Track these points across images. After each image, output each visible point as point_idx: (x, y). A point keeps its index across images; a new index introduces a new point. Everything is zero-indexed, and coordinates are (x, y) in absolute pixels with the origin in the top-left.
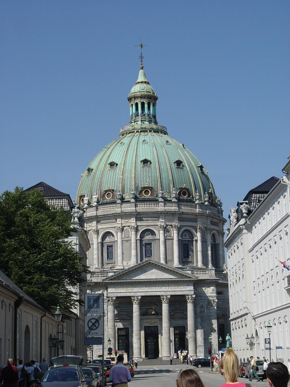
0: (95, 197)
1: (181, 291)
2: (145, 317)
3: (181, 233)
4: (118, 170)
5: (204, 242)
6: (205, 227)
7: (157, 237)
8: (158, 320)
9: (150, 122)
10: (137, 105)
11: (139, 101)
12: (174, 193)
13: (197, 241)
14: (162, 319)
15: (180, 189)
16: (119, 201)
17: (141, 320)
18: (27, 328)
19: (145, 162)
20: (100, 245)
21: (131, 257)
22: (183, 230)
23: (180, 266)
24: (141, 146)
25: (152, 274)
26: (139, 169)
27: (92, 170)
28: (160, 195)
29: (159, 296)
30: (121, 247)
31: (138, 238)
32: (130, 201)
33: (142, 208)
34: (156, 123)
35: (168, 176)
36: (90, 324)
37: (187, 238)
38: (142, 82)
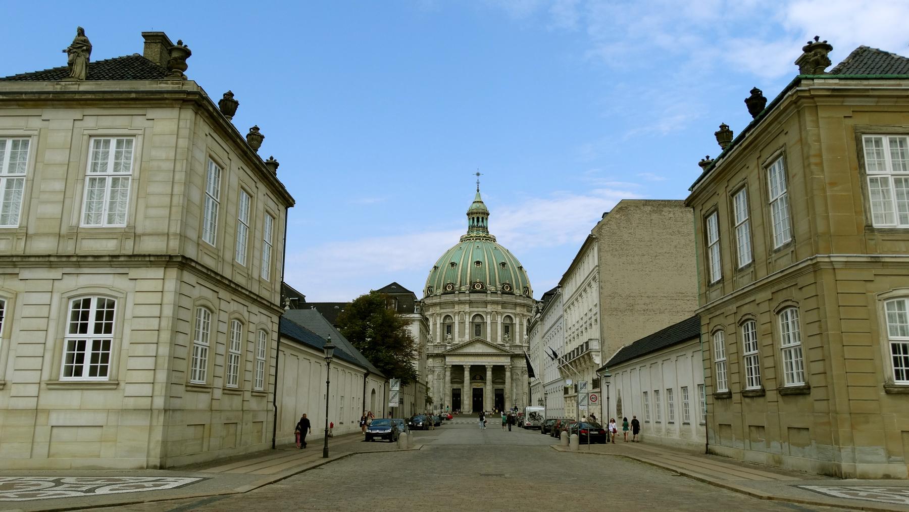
2: (473, 381)
3: (503, 318)
5: (521, 324)
7: (485, 321)
8: (483, 384)
9: (483, 232)
10: (473, 218)
11: (475, 216)
12: (499, 287)
13: (515, 324)
15: (503, 284)
16: (457, 292)
17: (471, 383)
19: (478, 263)
20: (442, 324)
21: (465, 335)
25: (479, 348)
29: (485, 366)
31: (471, 320)
33: (474, 297)
34: (488, 232)
36: (392, 395)
37: (508, 321)
38: (478, 202)
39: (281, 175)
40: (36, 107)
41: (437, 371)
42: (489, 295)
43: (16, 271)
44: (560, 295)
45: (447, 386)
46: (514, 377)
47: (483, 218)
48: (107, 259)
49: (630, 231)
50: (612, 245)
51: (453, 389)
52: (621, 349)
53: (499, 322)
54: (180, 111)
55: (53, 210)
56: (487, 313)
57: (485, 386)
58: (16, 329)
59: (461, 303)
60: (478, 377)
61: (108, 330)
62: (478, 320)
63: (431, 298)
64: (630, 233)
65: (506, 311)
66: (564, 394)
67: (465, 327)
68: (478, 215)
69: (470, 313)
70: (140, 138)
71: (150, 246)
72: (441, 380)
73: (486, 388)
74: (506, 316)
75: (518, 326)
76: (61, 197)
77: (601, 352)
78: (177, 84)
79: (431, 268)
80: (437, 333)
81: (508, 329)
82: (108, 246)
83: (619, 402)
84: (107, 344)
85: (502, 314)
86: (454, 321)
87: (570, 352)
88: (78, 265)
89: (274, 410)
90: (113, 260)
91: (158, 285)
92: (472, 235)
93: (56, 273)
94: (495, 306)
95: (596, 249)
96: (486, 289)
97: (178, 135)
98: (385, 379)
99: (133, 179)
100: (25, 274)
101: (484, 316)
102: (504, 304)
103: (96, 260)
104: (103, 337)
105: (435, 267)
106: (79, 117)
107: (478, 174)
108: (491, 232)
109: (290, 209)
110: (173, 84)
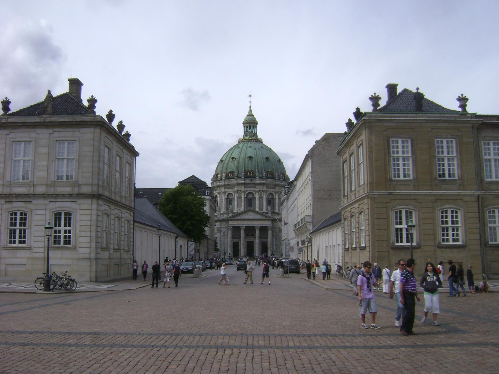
0: (224, 175)
1: (265, 224)
3: (267, 195)
4: (236, 162)
6: (280, 192)
7: (255, 197)
8: (254, 239)
12: (264, 174)
13: (275, 198)
14: (255, 238)
15: (267, 172)
16: (236, 178)
17: (245, 238)
18: (181, 246)
19: (250, 158)
20: (226, 199)
21: (241, 206)
22: (268, 193)
23: (266, 211)
24: (248, 149)
26: (247, 162)
27: (223, 160)
28: (257, 175)
30: (237, 201)
31: (245, 197)
32: (241, 178)
33: (248, 181)
34: (257, 136)
35: (262, 165)
37: (271, 197)
38: (250, 115)
39: (132, 142)
40: (33, 128)
41: (224, 230)
42: (258, 179)
43: (31, 200)
44: (296, 185)
45: (229, 240)
46: (274, 234)
47: (253, 127)
48: (68, 196)
49: (330, 152)
50: (320, 160)
51: (234, 242)
52: (323, 221)
54: (94, 129)
55: (43, 174)
56: (256, 192)
57: (255, 240)
58: (33, 224)
59: (238, 184)
61: (70, 225)
62: (250, 196)
63: (218, 182)
64: (330, 153)
65: (269, 190)
66: (297, 246)
67: (241, 201)
68: (250, 124)
69: (245, 192)
70: (78, 142)
71: (86, 189)
72: (226, 237)
73: (255, 241)
74: (268, 194)
75: (277, 200)
76: (46, 168)
77: (312, 223)
78: (92, 117)
79: (219, 160)
80: (223, 205)
81: (271, 202)
82: (67, 190)
83: (318, 251)
84: (70, 231)
85: (266, 192)
86: (234, 197)
87: (298, 221)
88: (56, 198)
89: (133, 258)
91: (89, 207)
92: (246, 138)
93: (47, 202)
94: (262, 187)
95: (310, 162)
96: (256, 175)
97: (94, 140)
98: (187, 239)
99: (76, 160)
100: (35, 202)
101: (255, 194)
102: (268, 186)
104: (68, 228)
105: (221, 161)
106: (51, 132)
107: (250, 96)
108: (260, 135)
109: (137, 158)
110: (91, 117)
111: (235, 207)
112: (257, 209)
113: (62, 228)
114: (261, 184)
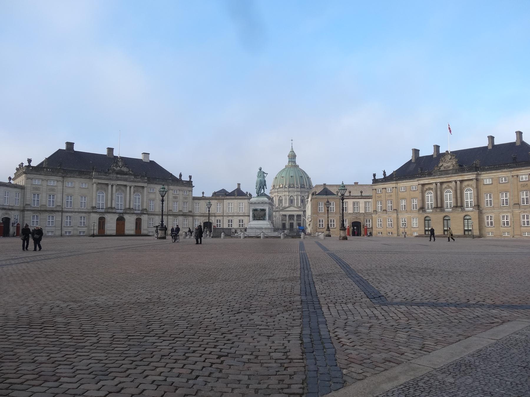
16: (284, 188)
17: (289, 221)
19: (292, 176)
34: (296, 163)
37: (303, 198)
53: (299, 199)
59: (285, 191)
60: (292, 219)
62: (291, 198)
65: (302, 194)
69: (289, 195)
79: (274, 177)
82: (242, 214)
90: (243, 216)
103: (241, 216)
105: (276, 178)
108: (298, 163)
111: (284, 204)
112: (296, 205)
113: (241, 223)
114: (297, 191)
